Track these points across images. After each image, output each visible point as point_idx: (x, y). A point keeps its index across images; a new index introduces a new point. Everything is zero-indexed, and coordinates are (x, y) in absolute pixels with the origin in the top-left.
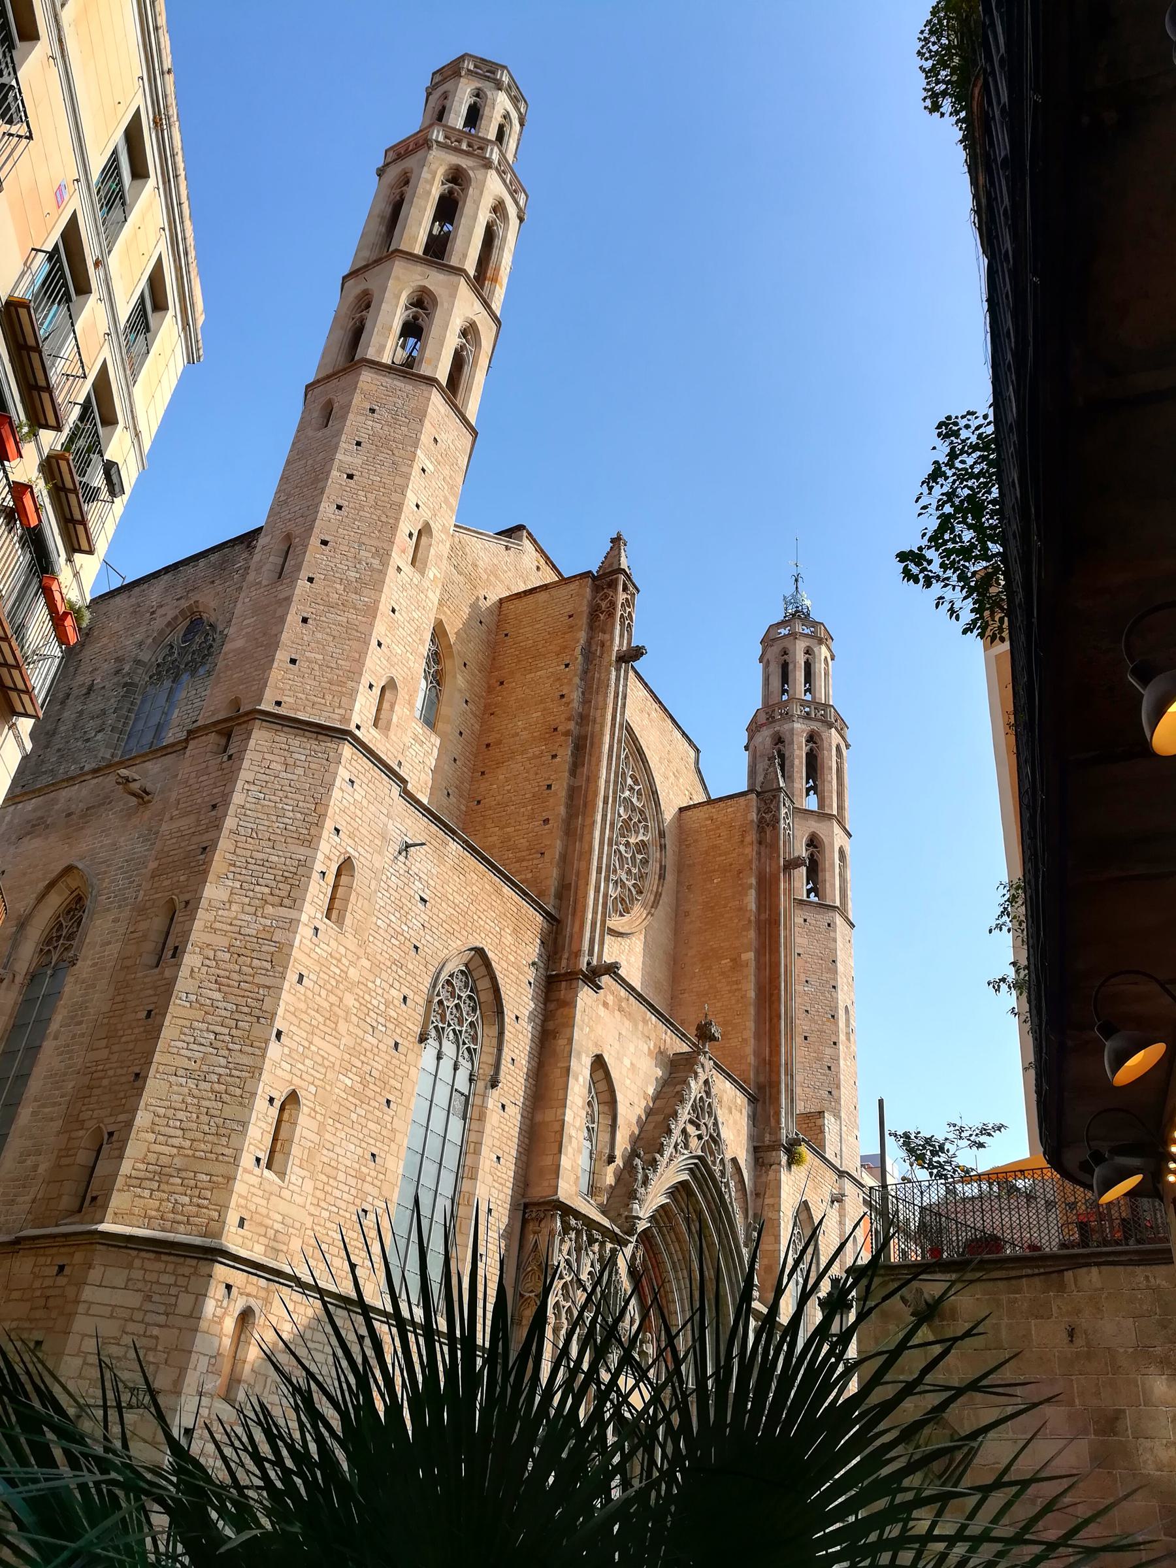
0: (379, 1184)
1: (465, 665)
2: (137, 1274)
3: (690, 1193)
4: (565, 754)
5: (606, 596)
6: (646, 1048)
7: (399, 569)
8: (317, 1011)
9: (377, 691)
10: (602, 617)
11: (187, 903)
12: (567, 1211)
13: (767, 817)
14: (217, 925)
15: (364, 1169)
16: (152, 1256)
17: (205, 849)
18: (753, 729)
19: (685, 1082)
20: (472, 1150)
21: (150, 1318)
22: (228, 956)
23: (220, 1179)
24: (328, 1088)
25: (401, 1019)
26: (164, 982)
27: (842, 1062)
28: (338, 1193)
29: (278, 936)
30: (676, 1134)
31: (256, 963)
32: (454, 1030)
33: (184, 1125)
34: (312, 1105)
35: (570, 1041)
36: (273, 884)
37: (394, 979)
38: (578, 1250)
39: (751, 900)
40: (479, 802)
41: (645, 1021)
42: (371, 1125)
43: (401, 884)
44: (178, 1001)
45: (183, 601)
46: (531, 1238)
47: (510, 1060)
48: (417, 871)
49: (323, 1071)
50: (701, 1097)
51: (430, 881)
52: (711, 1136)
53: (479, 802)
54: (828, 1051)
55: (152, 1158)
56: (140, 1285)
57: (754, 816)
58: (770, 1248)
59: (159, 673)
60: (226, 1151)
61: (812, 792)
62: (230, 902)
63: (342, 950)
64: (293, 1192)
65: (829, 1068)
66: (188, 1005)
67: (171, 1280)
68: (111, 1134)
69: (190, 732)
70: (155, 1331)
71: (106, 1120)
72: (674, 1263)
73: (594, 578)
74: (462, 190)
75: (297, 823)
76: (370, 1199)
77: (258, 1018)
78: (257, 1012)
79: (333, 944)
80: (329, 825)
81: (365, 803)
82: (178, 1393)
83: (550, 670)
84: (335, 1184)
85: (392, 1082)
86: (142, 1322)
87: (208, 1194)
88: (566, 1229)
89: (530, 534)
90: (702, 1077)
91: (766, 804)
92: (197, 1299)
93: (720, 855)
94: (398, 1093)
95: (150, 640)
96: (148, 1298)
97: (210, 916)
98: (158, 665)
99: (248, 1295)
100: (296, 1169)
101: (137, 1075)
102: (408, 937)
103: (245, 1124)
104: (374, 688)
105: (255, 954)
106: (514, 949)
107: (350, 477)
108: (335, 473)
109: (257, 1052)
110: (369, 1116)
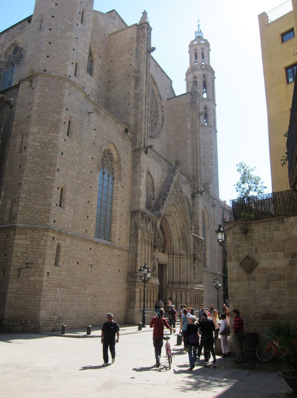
1: (100, 56)
2: (28, 236)
3: (176, 206)
4: (133, 83)
5: (142, 31)
6: (161, 168)
7: (77, 25)
8: (68, 163)
9: (74, 65)
12: (143, 214)
13: (193, 100)
14: (37, 140)
16: (31, 231)
17: (29, 117)
18: (187, 74)
19: (173, 177)
20: (115, 198)
21: (33, 247)
24: (74, 184)
26: (23, 157)
28: (80, 212)
29: (54, 142)
30: (171, 191)
32: (107, 167)
33: (35, 196)
35: (140, 168)
38: (146, 223)
39: (189, 125)
40: (108, 100)
41: (160, 161)
42: (87, 193)
43: (88, 125)
44: (28, 162)
45: (11, 41)
46: (134, 220)
48: (92, 121)
49: (71, 179)
50: (177, 181)
51: (96, 124)
53: (108, 100)
55: (27, 206)
56: (29, 239)
57: (189, 100)
58: (197, 219)
59: (7, 65)
60: (48, 203)
61: (205, 93)
62: (39, 132)
63: (73, 145)
64: (67, 212)
65: (211, 171)
66: (31, 163)
68: (15, 200)
69: (19, 82)
72: (171, 224)
73: (138, 26)
77: (52, 165)
78: (50, 164)
80: (65, 107)
82: (44, 264)
83: (126, 56)
85: (91, 181)
86: (31, 248)
87: (44, 215)
90: (177, 175)
92: (45, 242)
94: (93, 184)
95: (3, 55)
96: (32, 242)
97: (33, 137)
98: (7, 62)
99: (59, 240)
100: (68, 206)
101: (20, 183)
103: (52, 195)
104: (73, 64)
105: (48, 147)
106: (122, 143)
109: (53, 175)
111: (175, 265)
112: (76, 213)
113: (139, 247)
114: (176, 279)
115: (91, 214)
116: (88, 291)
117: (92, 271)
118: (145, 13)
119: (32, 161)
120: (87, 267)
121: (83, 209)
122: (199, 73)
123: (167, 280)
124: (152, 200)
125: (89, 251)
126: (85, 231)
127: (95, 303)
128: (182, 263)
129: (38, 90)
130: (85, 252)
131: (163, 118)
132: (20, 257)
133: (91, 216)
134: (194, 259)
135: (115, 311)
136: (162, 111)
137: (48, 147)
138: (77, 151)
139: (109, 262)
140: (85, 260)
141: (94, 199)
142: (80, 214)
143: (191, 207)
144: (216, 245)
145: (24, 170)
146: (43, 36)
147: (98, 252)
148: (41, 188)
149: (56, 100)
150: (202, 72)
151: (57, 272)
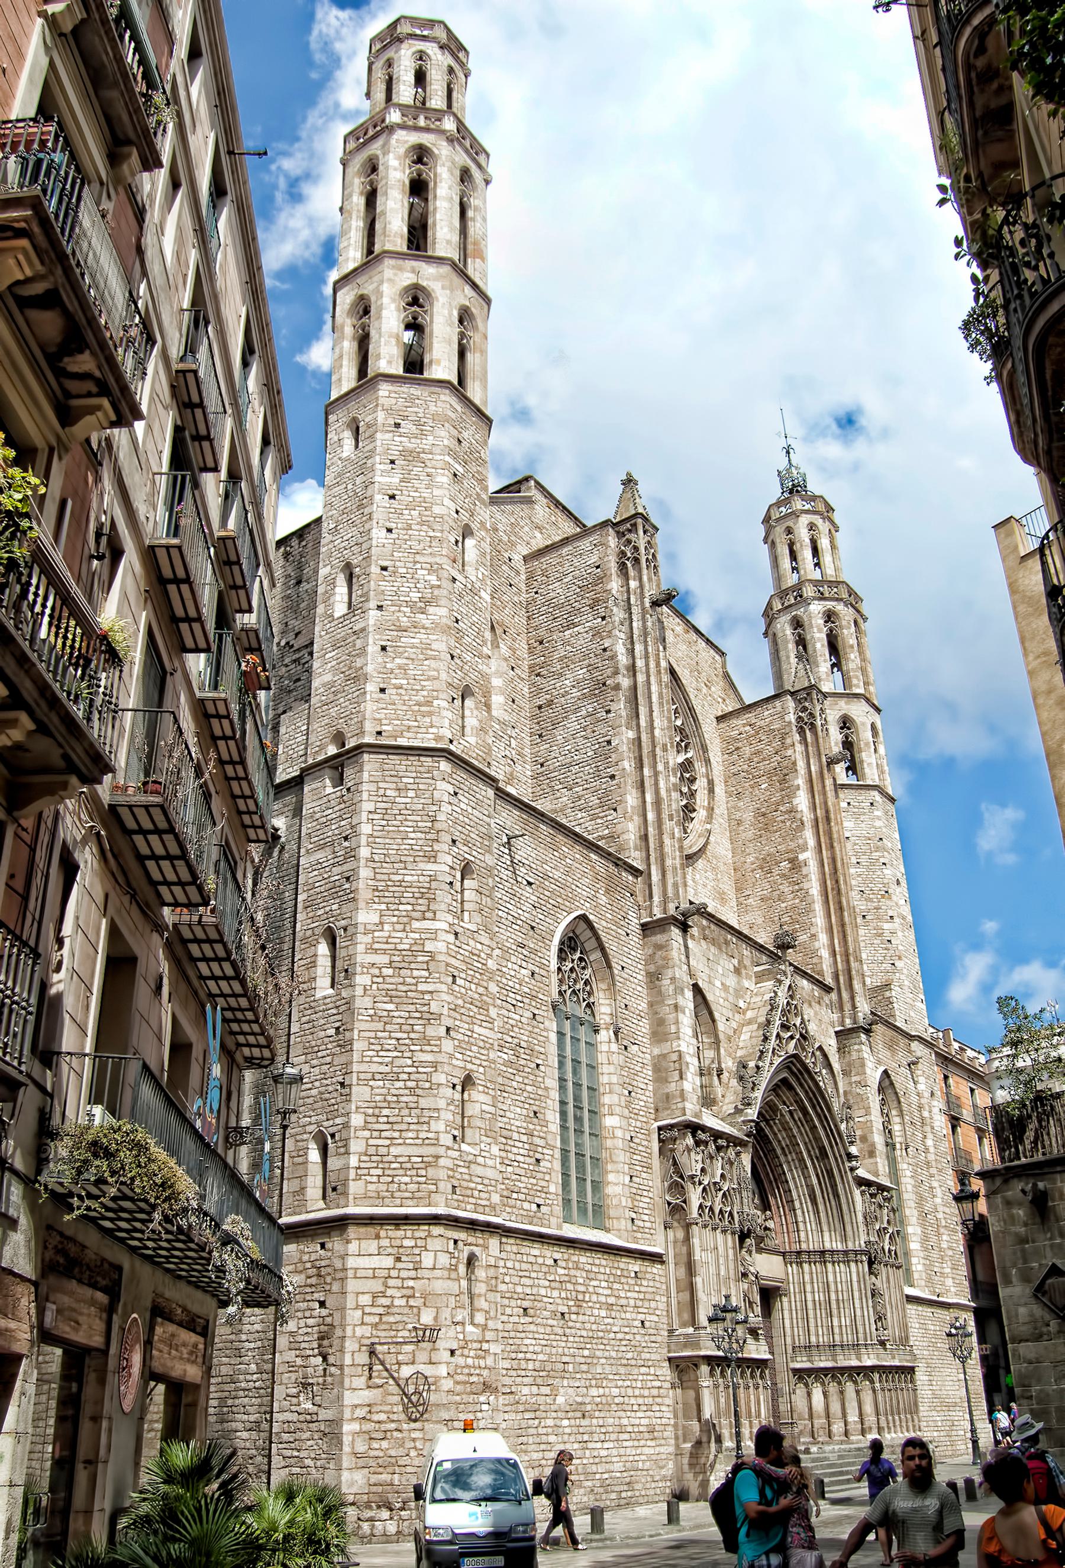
2: (385, 1242)
3: (791, 1088)
7: (454, 580)
11: (345, 930)
12: (694, 1128)
14: (376, 946)
15: (531, 1126)
21: (404, 1274)
22: (390, 972)
23: (430, 1159)
29: (429, 946)
31: (416, 973)
33: (391, 1120)
36: (412, 901)
42: (529, 1088)
52: (801, 1035)
54: (886, 926)
56: (390, 1250)
60: (430, 1135)
62: (382, 923)
63: (479, 946)
67: (411, 1243)
68: (333, 1136)
70: (411, 1283)
71: (325, 1124)
72: (783, 1149)
75: (420, 842)
79: (471, 942)
81: (470, 810)
87: (423, 1172)
88: (698, 1143)
89: (537, 483)
93: (764, 760)
96: (398, 1259)
97: (368, 939)
105: (413, 966)
107: (392, 497)
108: (378, 497)
109: (435, 1049)
111: (808, 1288)
113: (696, 1241)
114: (817, 1335)
115: (545, 1151)
116: (560, 1400)
117: (568, 1331)
118: (629, 482)
119: (371, 1012)
120: (555, 1323)
121: (524, 1138)
123: (789, 1340)
125: (552, 1270)
126: (534, 1207)
127: (586, 1437)
128: (831, 1278)
129: (365, 796)
130: (540, 1275)
131: (711, 783)
132: (367, 1310)
134: (871, 1263)
135: (643, 1457)
137: (413, 966)
138: (490, 962)
139: (612, 1300)
140: (545, 1299)
141: (549, 1102)
143: (840, 1078)
144: (938, 1200)
145: (351, 1042)
146: (363, 630)
147: (577, 1268)
148: (407, 1092)
149: (419, 818)
151: (476, 1345)
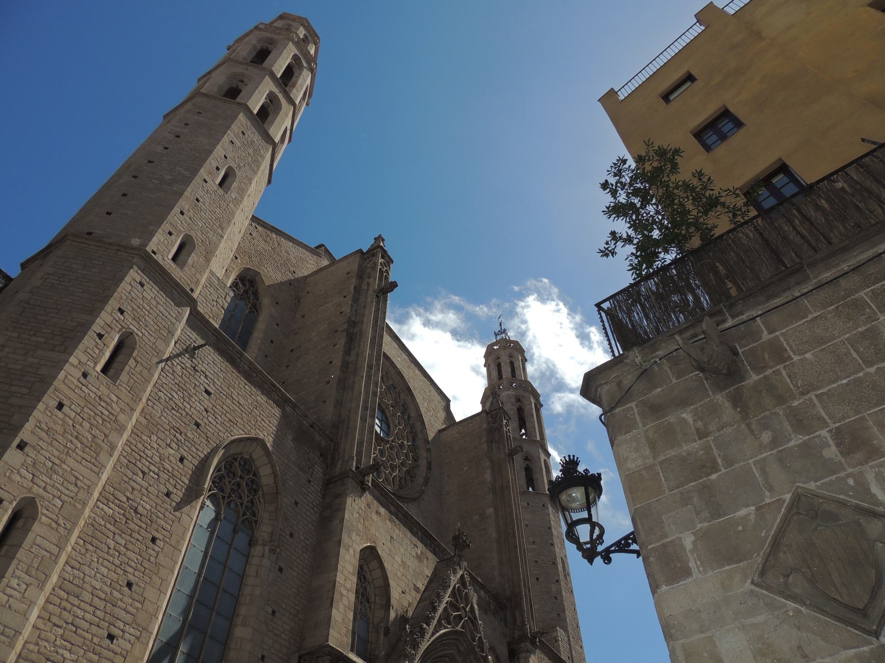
0: (134, 611)
4: (342, 342)
8: (76, 438)
10: (368, 271)
25: (176, 473)
27: (564, 593)
28: (80, 613)
34: (54, 517)
37: (172, 440)
39: (488, 476)
47: (288, 533)
49: (75, 490)
50: (459, 586)
52: (469, 618)
63: (115, 399)
64: (10, 596)
65: (556, 598)
74: (275, 47)
76: (121, 625)
84: (76, 602)
91: (493, 418)
94: (165, 533)
102: (191, 413)
110: (130, 546)
112: (57, 610)
122: (506, 395)
124: (382, 636)
133: (127, 636)
136: (426, 449)
142: (78, 622)
150: (513, 393)
